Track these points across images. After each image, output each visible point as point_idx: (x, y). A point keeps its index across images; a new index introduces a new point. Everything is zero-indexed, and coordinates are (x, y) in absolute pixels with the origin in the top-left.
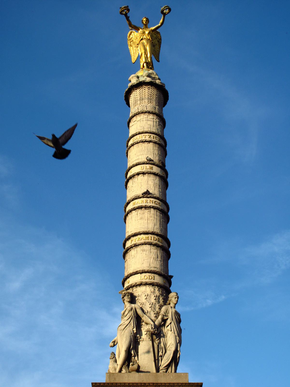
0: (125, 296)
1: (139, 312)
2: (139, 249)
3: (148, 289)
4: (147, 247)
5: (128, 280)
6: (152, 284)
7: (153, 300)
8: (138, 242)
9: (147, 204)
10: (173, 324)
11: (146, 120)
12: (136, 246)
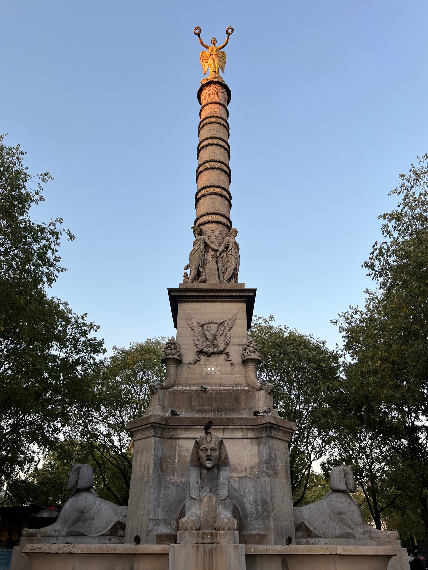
0: (195, 230)
1: (207, 241)
2: (207, 197)
3: (214, 226)
4: (213, 196)
6: (217, 222)
7: (217, 233)
8: (206, 193)
9: (213, 166)
10: (233, 249)
11: (213, 108)
12: (205, 195)
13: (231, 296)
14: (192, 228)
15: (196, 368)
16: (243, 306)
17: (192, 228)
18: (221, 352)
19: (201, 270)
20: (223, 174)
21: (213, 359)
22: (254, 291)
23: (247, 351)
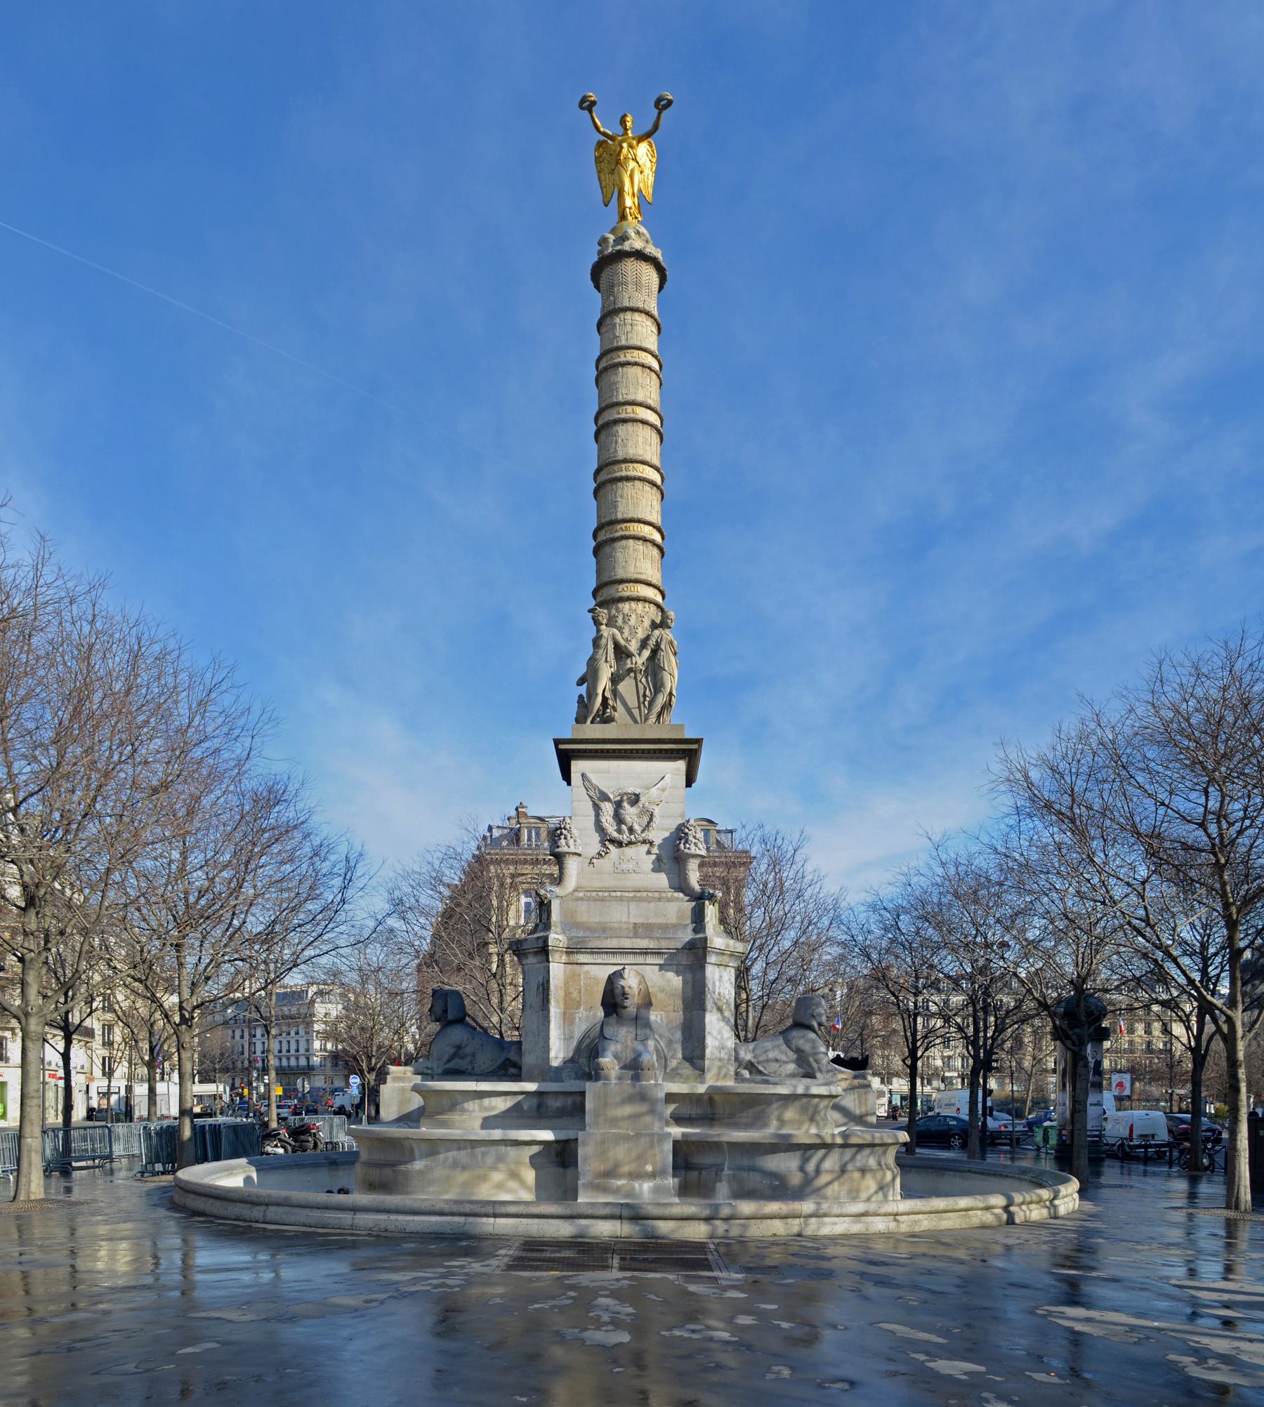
5: (600, 593)
13: (660, 751)
14: (590, 611)
15: (604, 864)
16: (681, 765)
17: (590, 611)
18: (644, 842)
19: (608, 694)
20: (648, 489)
21: (629, 851)
22: (698, 741)
23: (683, 841)
